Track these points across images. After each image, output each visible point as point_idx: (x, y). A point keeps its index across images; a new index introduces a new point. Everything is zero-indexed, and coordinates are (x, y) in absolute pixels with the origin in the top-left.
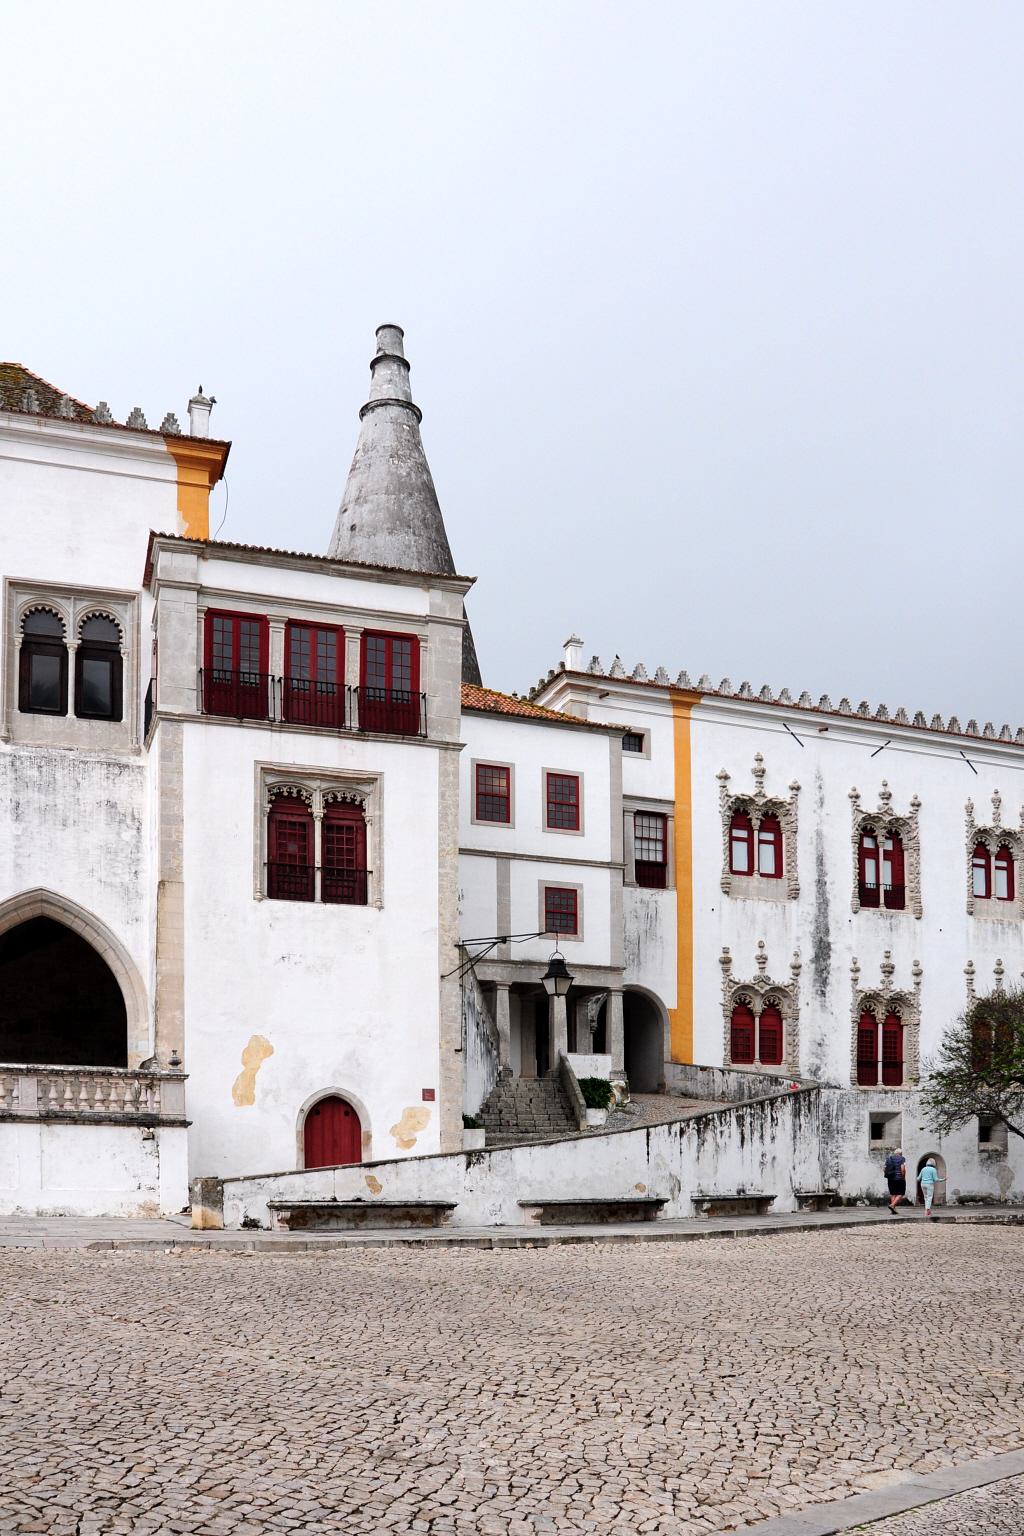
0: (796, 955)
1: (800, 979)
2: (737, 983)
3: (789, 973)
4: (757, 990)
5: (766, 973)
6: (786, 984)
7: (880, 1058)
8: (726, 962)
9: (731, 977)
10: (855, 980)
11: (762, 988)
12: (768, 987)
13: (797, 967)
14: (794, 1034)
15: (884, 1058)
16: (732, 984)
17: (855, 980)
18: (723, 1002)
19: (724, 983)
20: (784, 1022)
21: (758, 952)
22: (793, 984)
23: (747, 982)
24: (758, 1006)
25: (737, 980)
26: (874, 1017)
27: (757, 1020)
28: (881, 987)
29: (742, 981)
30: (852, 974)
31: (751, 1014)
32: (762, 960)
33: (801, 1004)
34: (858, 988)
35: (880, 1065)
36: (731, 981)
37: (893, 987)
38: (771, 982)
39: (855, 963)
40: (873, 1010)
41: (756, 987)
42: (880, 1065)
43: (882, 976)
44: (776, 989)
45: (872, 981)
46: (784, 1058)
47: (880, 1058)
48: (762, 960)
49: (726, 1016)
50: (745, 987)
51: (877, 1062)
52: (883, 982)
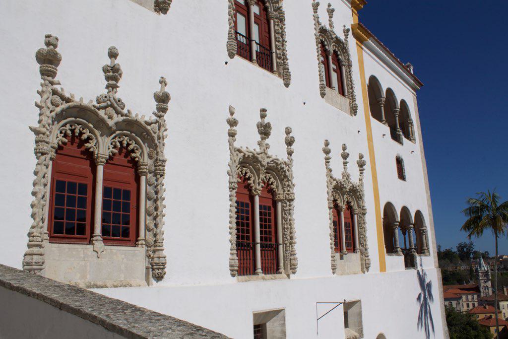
0: (163, 82)
1: (167, 116)
2: (68, 100)
3: (154, 104)
4: (102, 121)
5: (119, 94)
6: (147, 119)
7: (258, 240)
8: (48, 60)
9: (58, 88)
10: (232, 135)
11: (110, 118)
12: (120, 119)
13: (163, 99)
14: (156, 198)
15: (261, 239)
16: (57, 99)
17: (232, 135)
18: (36, 125)
19: (41, 93)
20: (143, 179)
21: (108, 62)
22: (157, 122)
23: (86, 102)
24: (103, 147)
25: (67, 95)
26: (248, 187)
27: (100, 169)
28: (258, 150)
29: (77, 99)
30: (228, 127)
31: (90, 156)
32: (113, 74)
33: (170, 151)
34: (237, 145)
35: (258, 247)
36: (55, 92)
37: (270, 152)
38: (125, 111)
39: (232, 114)
40: (249, 179)
41: (101, 113)
42: (258, 247)
43: (258, 137)
44: (132, 126)
45: (249, 141)
46: (142, 236)
47: (258, 240)
48: (113, 74)
49: (39, 153)
50: (81, 111)
51: (255, 244)
52: (259, 144)
